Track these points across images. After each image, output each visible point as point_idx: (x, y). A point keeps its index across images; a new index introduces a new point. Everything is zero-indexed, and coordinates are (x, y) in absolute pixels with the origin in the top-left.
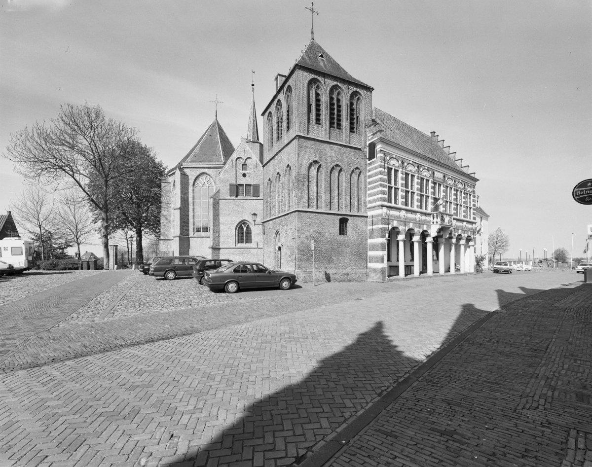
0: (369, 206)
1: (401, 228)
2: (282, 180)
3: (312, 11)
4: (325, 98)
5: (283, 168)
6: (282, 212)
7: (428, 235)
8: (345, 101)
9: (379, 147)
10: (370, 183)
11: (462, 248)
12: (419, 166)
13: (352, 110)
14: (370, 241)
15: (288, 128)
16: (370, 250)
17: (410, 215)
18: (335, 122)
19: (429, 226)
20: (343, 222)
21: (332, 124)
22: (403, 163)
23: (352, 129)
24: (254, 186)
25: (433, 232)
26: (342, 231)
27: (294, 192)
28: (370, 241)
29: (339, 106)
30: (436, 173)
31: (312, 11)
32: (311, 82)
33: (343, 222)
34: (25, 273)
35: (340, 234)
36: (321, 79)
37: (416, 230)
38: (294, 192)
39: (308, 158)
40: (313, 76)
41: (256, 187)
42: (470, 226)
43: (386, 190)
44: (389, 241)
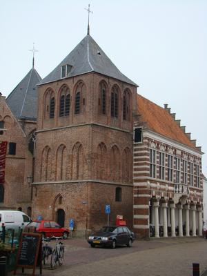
0: (134, 178)
1: (157, 197)
2: (67, 152)
3: (89, 11)
4: (109, 95)
5: (71, 143)
6: (67, 179)
7: (172, 202)
8: (121, 95)
9: (145, 134)
10: (136, 160)
11: (194, 213)
12: (167, 146)
13: (125, 102)
14: (135, 207)
15: (77, 111)
16: (135, 214)
17: (163, 187)
18: (114, 113)
19: (173, 195)
20: (118, 190)
21: (112, 115)
22: (158, 145)
23: (124, 119)
24: (10, 144)
25: (176, 200)
26: (118, 198)
27: (86, 167)
28: (135, 207)
29: (116, 99)
30: (177, 151)
31: (89, 11)
32: (102, 83)
33: (118, 190)
34: (138, 219)
35: (116, 200)
36: (107, 80)
37: (166, 198)
38: (86, 167)
39: (98, 140)
40: (102, 78)
41: (13, 146)
42: (199, 194)
43: (149, 167)
44: (151, 207)
